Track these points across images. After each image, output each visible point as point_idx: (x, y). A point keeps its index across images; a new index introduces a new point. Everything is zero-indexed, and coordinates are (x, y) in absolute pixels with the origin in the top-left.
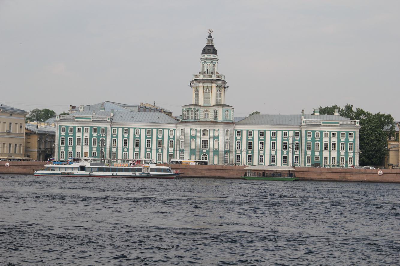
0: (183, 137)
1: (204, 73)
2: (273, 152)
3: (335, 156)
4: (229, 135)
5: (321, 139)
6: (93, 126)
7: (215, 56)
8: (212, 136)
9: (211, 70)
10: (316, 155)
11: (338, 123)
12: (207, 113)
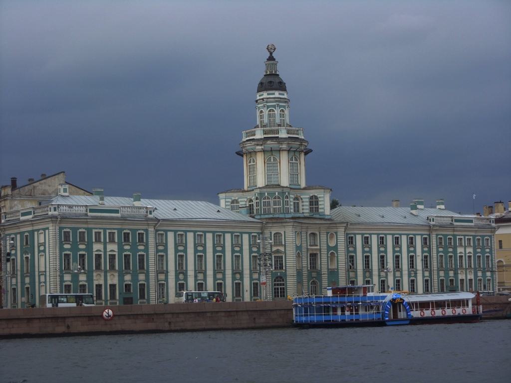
0: (282, 249)
1: (265, 126)
2: (398, 274)
3: (472, 277)
5: (455, 248)
6: (124, 227)
8: (324, 247)
9: (278, 121)
11: (471, 221)
12: (296, 201)
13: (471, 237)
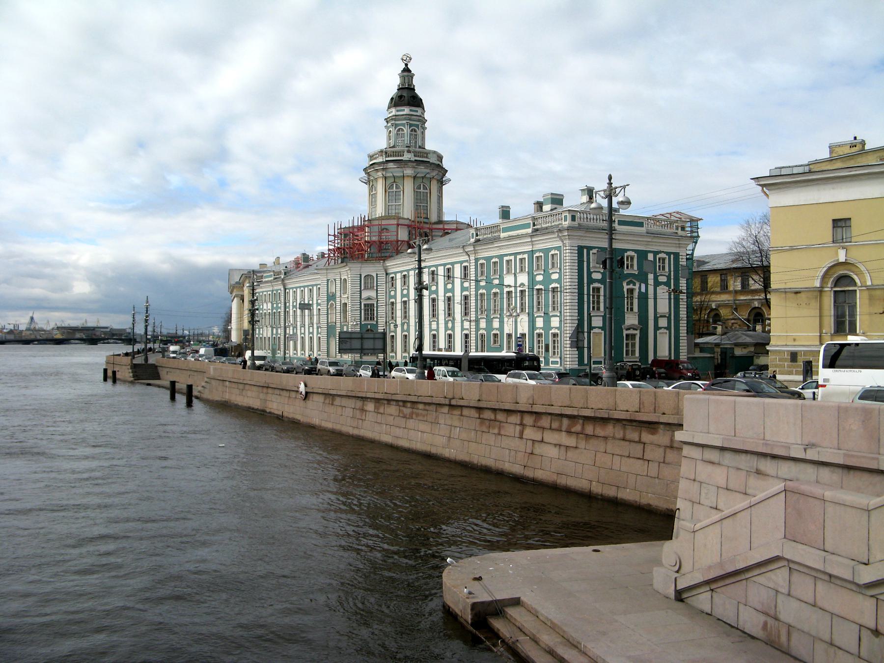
3: (526, 331)
4: (375, 288)
5: (501, 278)
7: (404, 110)
10: (494, 329)
13: (526, 256)
